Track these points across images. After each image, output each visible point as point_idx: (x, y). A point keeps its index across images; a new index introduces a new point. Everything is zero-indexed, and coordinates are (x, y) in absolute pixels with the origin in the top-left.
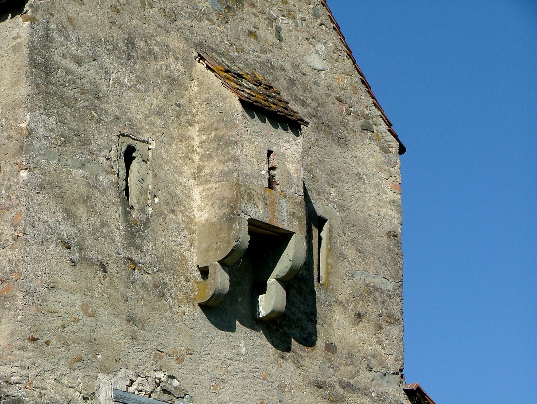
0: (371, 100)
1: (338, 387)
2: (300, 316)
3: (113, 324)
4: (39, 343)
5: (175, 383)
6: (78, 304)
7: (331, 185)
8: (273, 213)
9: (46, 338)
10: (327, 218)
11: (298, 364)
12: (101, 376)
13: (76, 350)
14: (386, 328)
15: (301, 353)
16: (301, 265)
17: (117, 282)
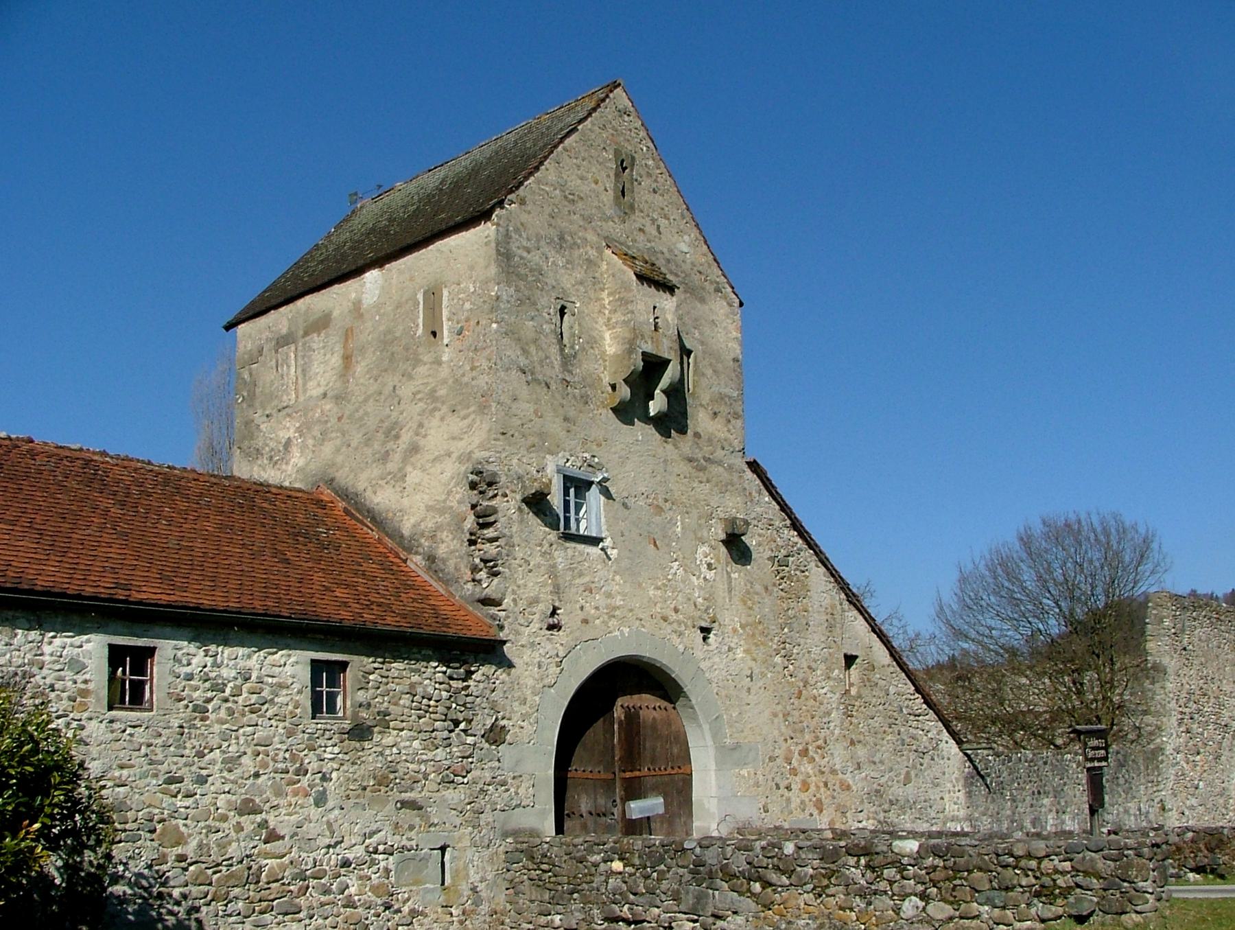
0: (720, 272)
1: (702, 461)
3: (554, 422)
4: (507, 435)
5: (596, 460)
6: (532, 410)
7: (695, 328)
8: (657, 347)
9: (511, 433)
12: (547, 456)
13: (531, 440)
14: (733, 421)
15: (677, 438)
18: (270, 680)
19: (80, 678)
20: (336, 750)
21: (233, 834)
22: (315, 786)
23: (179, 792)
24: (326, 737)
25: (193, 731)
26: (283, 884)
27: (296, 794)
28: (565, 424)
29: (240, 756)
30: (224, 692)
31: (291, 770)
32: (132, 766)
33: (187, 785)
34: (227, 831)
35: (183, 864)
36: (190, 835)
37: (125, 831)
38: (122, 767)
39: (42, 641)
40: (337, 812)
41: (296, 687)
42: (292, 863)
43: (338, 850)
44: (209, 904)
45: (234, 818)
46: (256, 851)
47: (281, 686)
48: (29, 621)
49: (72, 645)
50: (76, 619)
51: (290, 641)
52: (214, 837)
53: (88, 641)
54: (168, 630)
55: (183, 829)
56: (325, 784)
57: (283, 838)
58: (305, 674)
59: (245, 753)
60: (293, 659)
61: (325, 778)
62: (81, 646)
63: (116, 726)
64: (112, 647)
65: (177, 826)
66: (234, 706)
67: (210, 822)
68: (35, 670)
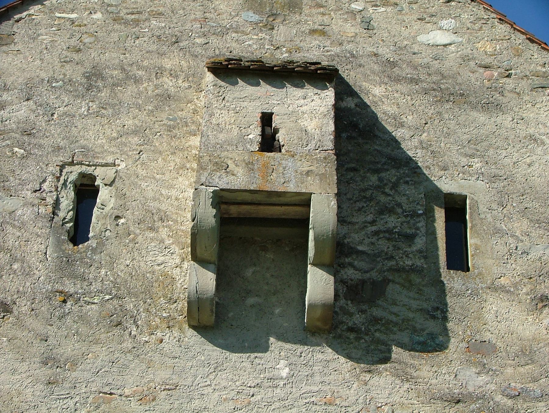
1: (498, 398)
2: (411, 315)
3: (14, 371)
7: (472, 156)
10: (464, 193)
11: (407, 378)
16: (333, 230)
17: (30, 322)
28: (45, 372)
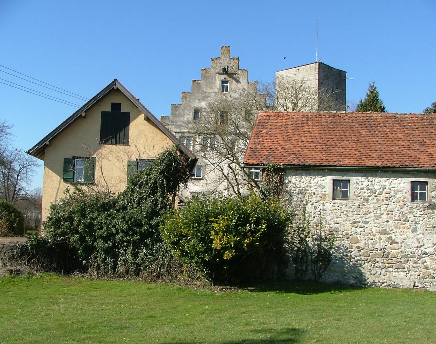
18: (393, 189)
19: (323, 190)
20: (422, 213)
21: (378, 241)
22: (412, 226)
23: (358, 226)
24: (417, 208)
25: (363, 207)
26: (398, 259)
27: (404, 228)
29: (381, 215)
30: (375, 193)
31: (402, 220)
32: (341, 218)
33: (361, 224)
34: (376, 240)
35: (359, 249)
36: (361, 240)
37: (338, 237)
38: (337, 218)
39: (311, 180)
40: (421, 235)
41: (405, 191)
42: (401, 252)
43: (422, 248)
44: (368, 263)
45: (378, 235)
46: (387, 247)
47: (398, 191)
48: (306, 174)
49: (320, 180)
50: (321, 172)
51: (402, 175)
52: (370, 241)
53: (326, 179)
54: (354, 174)
55: (359, 238)
56: (417, 225)
57: (398, 243)
58: (409, 187)
59: (383, 214)
60: (403, 181)
61: (416, 223)
62: (324, 181)
63: (335, 205)
64: (334, 180)
65: (357, 237)
66: (379, 198)
67: (369, 236)
68: (309, 188)
